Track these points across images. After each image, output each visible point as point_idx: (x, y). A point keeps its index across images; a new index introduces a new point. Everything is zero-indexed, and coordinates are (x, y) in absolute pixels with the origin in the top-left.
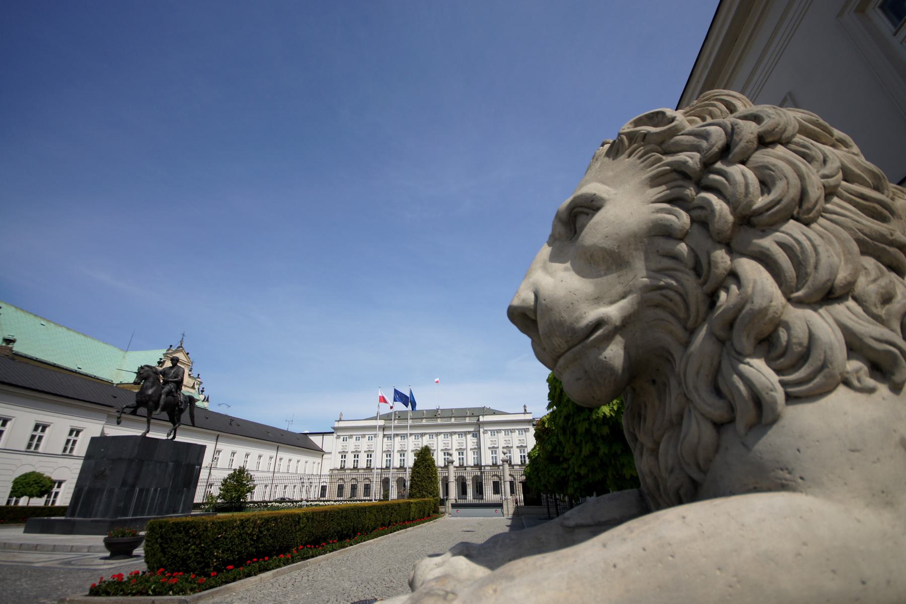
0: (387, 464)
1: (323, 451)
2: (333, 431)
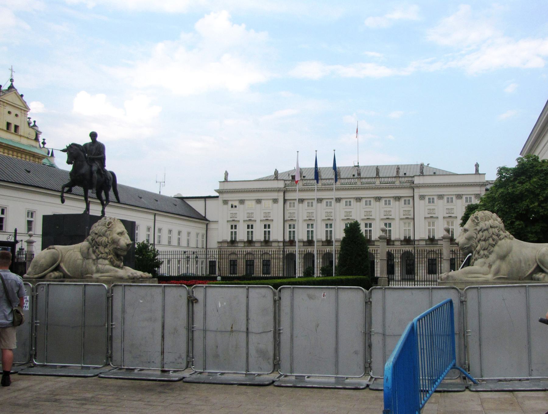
0: (290, 237)
1: (207, 220)
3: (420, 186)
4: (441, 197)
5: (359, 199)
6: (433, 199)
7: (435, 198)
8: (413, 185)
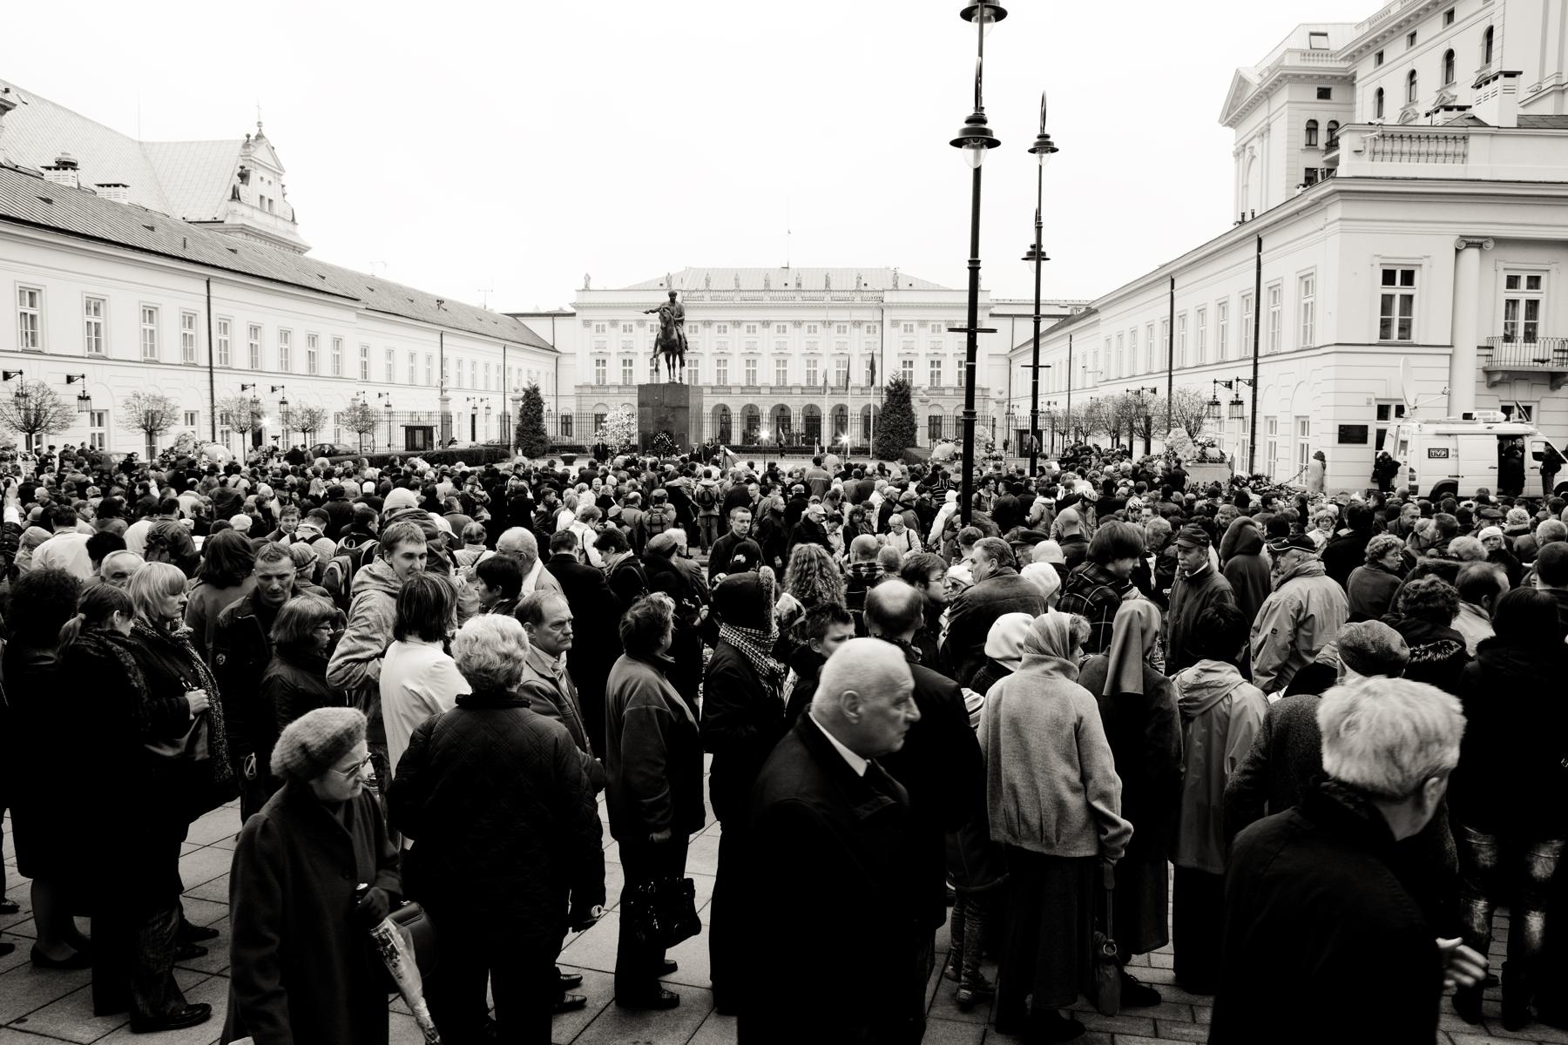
2: (573, 310)
3: (891, 307)
4: (923, 323)
5: (798, 324)
6: (911, 326)
7: (915, 325)
8: (881, 304)
